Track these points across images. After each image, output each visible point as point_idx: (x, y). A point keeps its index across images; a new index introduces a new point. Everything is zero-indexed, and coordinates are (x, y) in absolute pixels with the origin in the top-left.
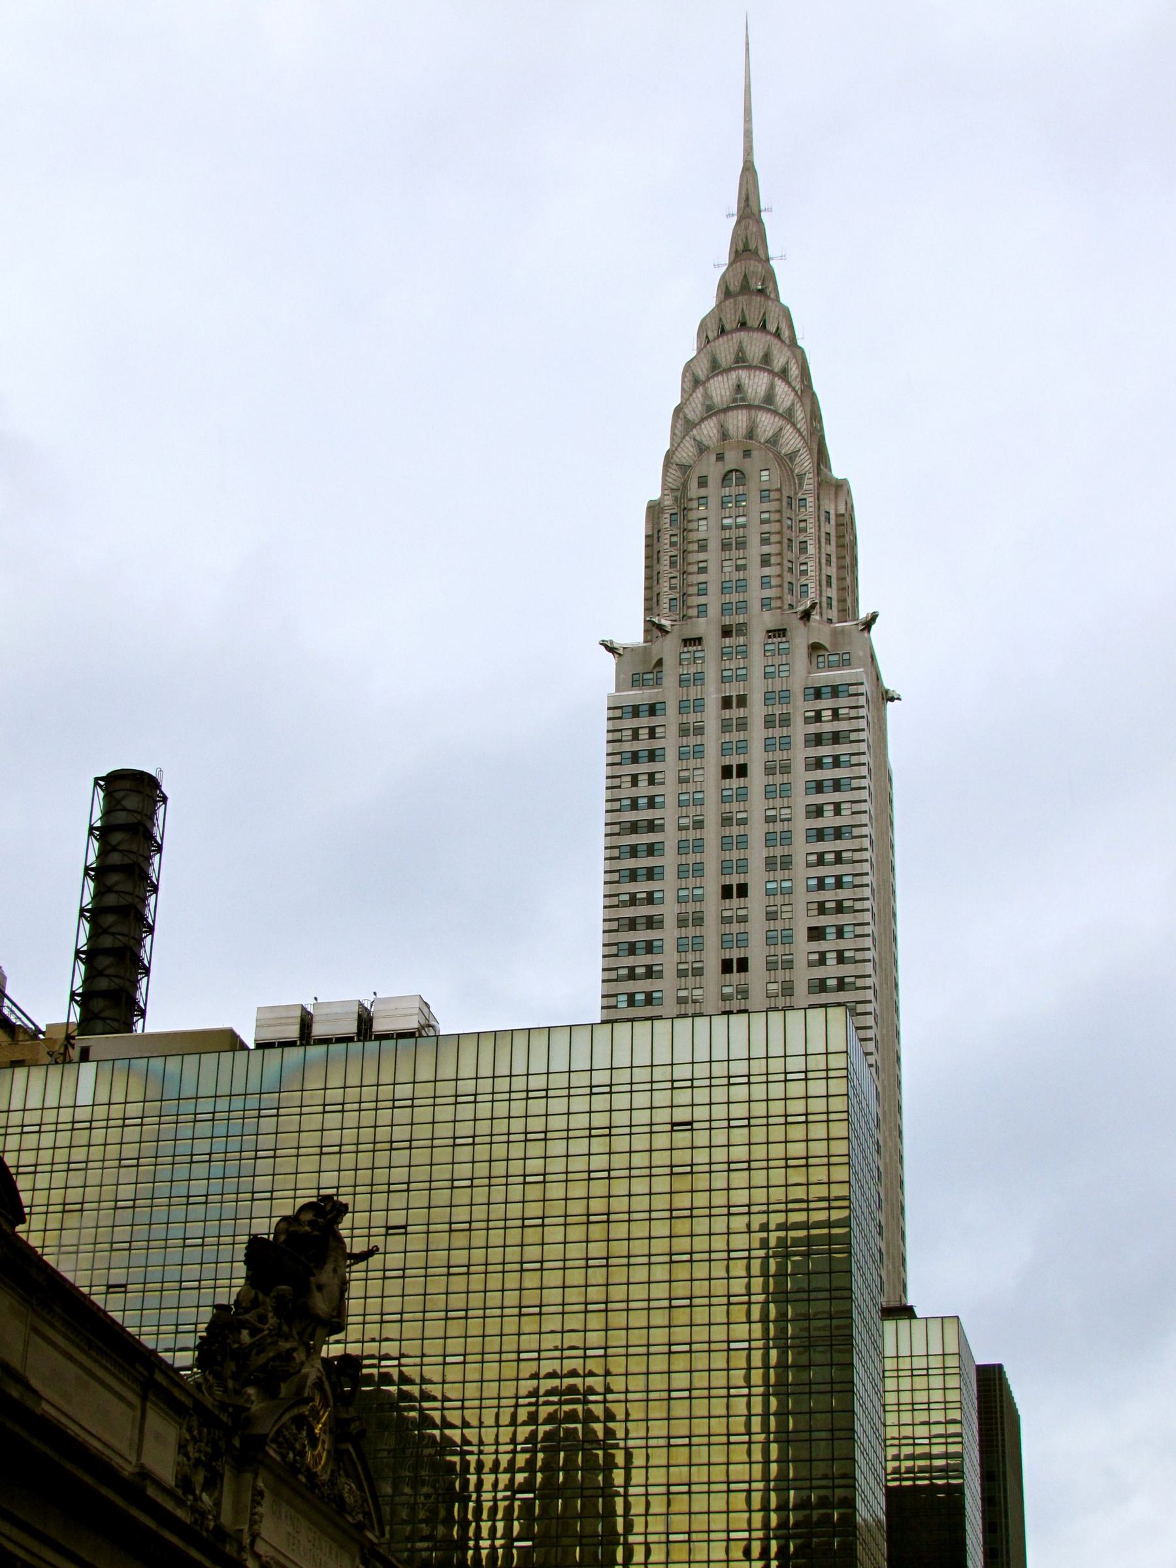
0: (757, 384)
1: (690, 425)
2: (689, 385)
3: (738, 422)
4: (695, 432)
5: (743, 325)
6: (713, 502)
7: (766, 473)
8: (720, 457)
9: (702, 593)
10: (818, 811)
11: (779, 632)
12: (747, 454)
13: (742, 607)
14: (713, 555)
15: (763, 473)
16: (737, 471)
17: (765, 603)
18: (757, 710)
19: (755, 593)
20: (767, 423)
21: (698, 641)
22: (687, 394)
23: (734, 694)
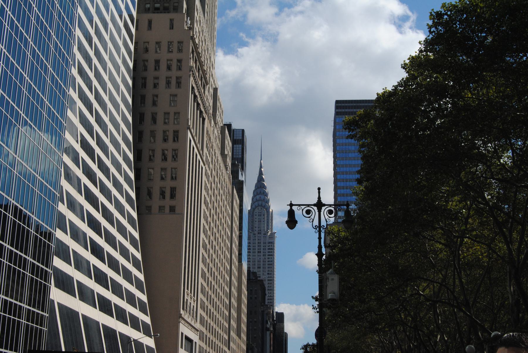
0: (262, 197)
3: (260, 203)
10: (269, 258)
11: (265, 234)
14: (257, 223)
18: (262, 245)
20: (264, 204)
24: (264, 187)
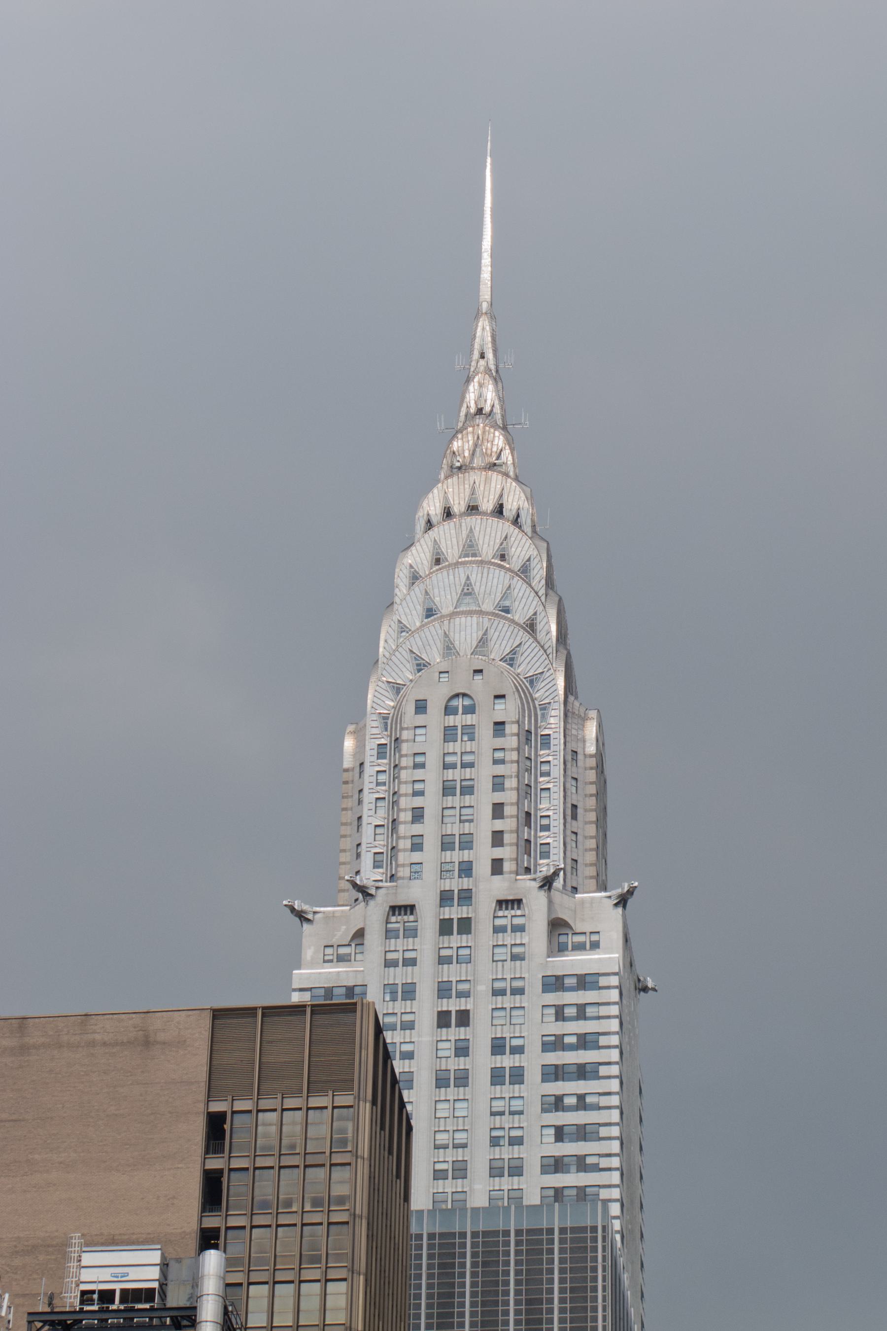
5: (473, 509)
9: (417, 846)
13: (466, 869)
17: (497, 866)
19: (482, 854)
21: (410, 909)
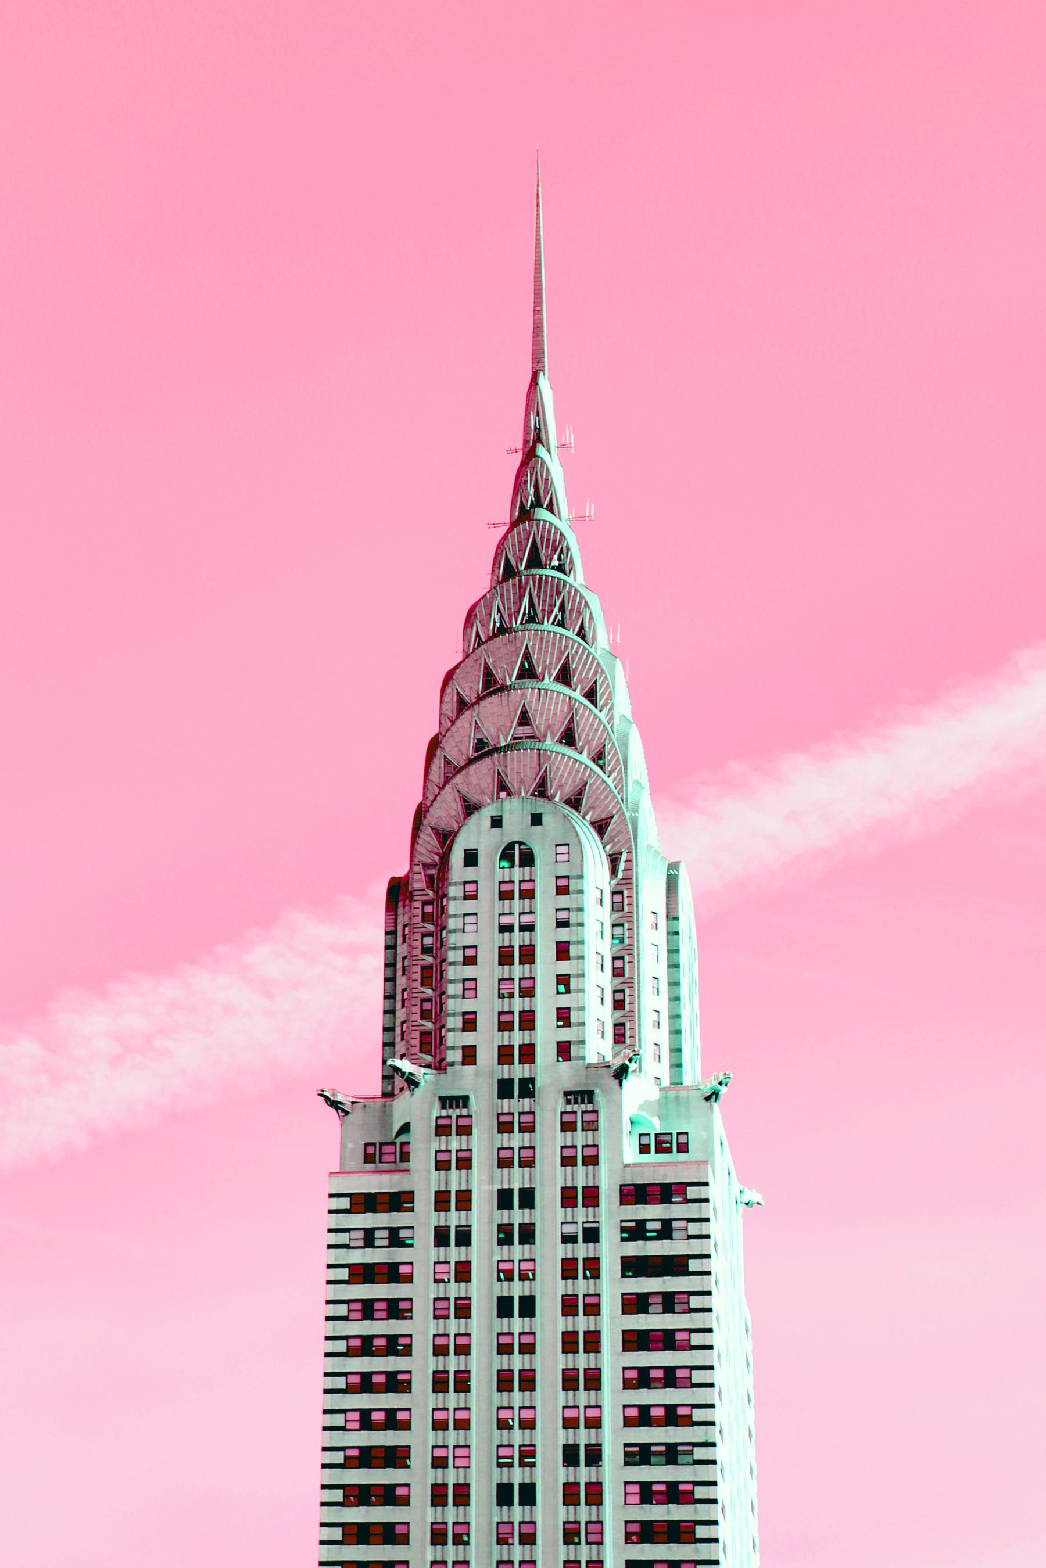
1: (453, 770)
2: (450, 707)
4: (458, 779)
6: (487, 892)
7: (564, 849)
8: (497, 822)
12: (536, 819)
13: (528, 1053)
14: (487, 971)
15: (560, 849)
16: (521, 843)
17: (564, 1050)
21: (462, 1101)
22: (448, 722)
23: (516, 1186)
24: (569, 612)
